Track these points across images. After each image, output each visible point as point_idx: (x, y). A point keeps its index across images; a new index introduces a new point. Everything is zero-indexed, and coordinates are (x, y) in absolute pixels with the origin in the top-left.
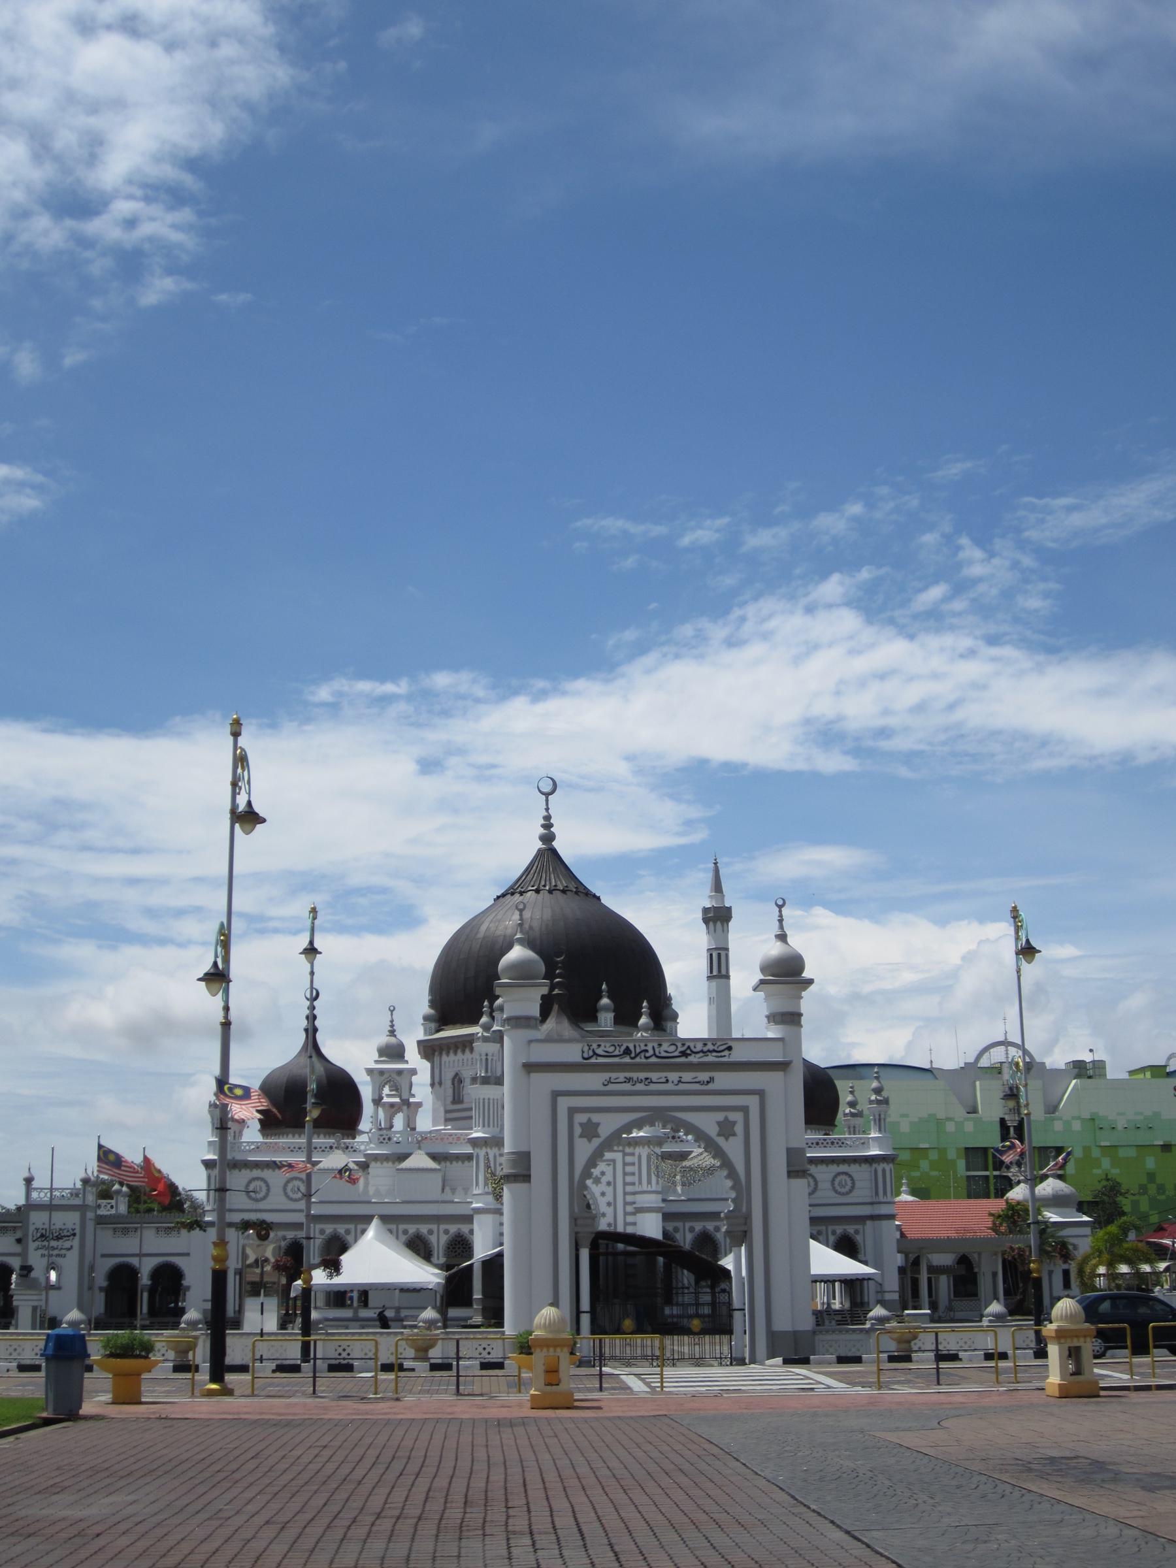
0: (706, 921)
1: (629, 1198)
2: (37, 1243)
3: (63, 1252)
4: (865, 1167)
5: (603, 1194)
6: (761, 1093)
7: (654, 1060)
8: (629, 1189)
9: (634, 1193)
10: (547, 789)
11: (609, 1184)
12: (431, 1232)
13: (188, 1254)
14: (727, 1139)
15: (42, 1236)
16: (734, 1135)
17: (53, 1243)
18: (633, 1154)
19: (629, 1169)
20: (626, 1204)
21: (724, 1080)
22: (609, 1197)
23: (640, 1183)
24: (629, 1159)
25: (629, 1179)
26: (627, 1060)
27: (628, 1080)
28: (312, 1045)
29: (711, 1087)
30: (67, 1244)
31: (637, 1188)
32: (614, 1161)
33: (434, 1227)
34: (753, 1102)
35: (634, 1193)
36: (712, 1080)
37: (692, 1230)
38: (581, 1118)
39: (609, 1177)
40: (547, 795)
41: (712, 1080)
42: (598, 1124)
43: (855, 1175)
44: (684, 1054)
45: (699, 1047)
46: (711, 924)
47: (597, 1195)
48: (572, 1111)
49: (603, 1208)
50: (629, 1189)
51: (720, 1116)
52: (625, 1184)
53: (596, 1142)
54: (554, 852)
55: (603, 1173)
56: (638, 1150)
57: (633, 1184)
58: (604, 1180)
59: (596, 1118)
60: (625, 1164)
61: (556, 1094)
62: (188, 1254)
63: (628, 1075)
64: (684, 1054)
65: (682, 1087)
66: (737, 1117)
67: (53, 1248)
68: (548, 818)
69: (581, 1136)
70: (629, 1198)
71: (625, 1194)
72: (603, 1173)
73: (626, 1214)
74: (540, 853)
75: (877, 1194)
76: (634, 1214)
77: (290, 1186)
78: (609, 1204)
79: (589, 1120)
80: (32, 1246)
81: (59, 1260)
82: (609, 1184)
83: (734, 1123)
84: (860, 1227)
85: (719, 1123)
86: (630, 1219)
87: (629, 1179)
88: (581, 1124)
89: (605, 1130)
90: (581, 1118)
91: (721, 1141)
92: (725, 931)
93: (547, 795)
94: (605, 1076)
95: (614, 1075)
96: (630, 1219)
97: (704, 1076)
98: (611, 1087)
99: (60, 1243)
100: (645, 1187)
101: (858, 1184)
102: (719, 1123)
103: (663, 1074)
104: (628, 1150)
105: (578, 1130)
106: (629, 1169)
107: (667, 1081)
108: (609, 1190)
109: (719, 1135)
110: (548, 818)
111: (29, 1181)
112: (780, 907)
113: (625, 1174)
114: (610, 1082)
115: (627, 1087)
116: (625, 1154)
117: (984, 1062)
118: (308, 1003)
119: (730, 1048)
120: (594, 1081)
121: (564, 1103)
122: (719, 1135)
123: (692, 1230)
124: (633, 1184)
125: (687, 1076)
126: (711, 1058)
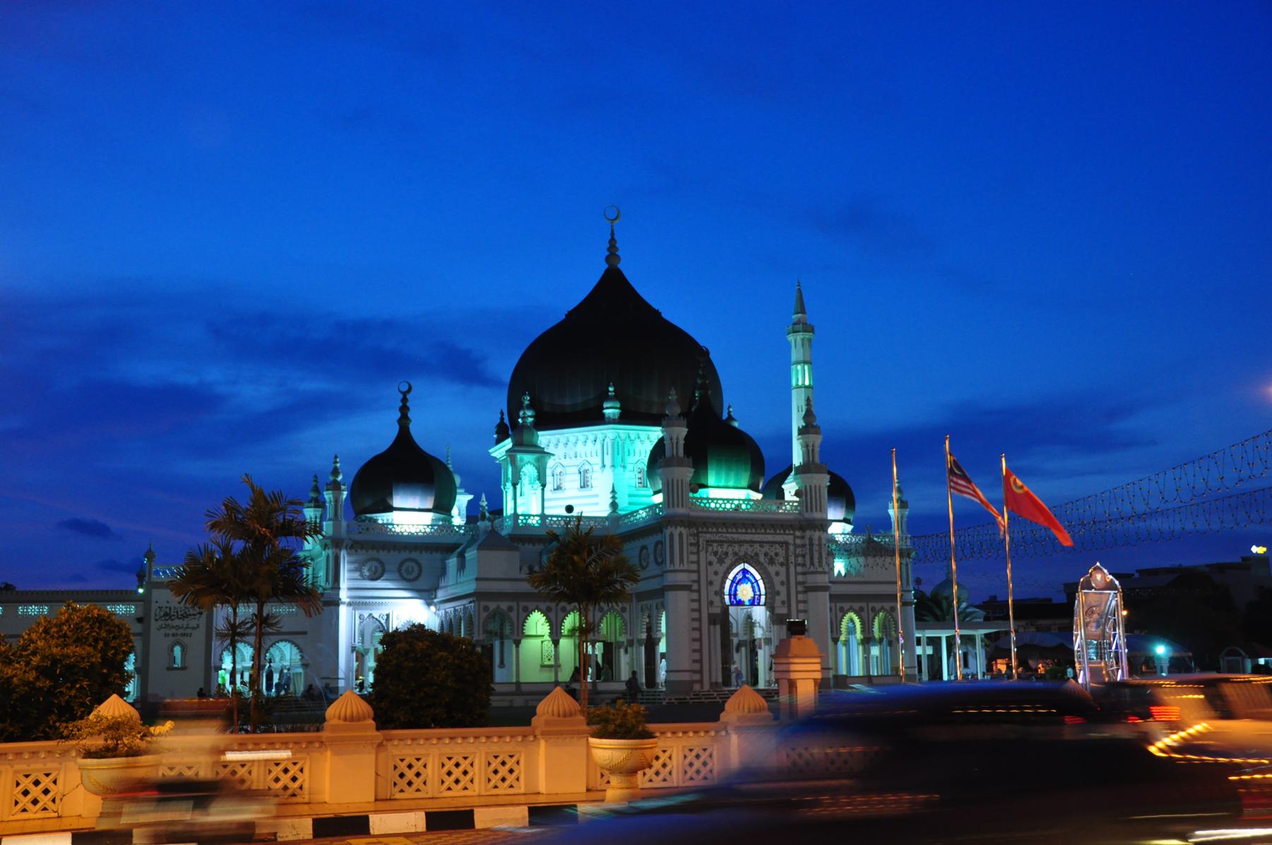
1: (800, 578)
2: (160, 622)
3: (188, 631)
9: (804, 574)
12: (510, 609)
13: (305, 633)
15: (166, 614)
17: (177, 622)
20: (798, 583)
22: (783, 577)
23: (812, 564)
28: (404, 436)
30: (193, 623)
32: (787, 543)
33: (514, 604)
35: (804, 574)
47: (773, 574)
55: (777, 554)
56: (808, 533)
62: (305, 633)
67: (178, 627)
71: (797, 574)
73: (797, 593)
74: (607, 272)
77: (416, 569)
78: (782, 583)
80: (154, 625)
81: (186, 640)
82: (782, 564)
86: (801, 597)
96: (801, 597)
99: (185, 622)
104: (798, 533)
106: (799, 551)
108: (783, 570)
116: (796, 537)
118: (401, 396)
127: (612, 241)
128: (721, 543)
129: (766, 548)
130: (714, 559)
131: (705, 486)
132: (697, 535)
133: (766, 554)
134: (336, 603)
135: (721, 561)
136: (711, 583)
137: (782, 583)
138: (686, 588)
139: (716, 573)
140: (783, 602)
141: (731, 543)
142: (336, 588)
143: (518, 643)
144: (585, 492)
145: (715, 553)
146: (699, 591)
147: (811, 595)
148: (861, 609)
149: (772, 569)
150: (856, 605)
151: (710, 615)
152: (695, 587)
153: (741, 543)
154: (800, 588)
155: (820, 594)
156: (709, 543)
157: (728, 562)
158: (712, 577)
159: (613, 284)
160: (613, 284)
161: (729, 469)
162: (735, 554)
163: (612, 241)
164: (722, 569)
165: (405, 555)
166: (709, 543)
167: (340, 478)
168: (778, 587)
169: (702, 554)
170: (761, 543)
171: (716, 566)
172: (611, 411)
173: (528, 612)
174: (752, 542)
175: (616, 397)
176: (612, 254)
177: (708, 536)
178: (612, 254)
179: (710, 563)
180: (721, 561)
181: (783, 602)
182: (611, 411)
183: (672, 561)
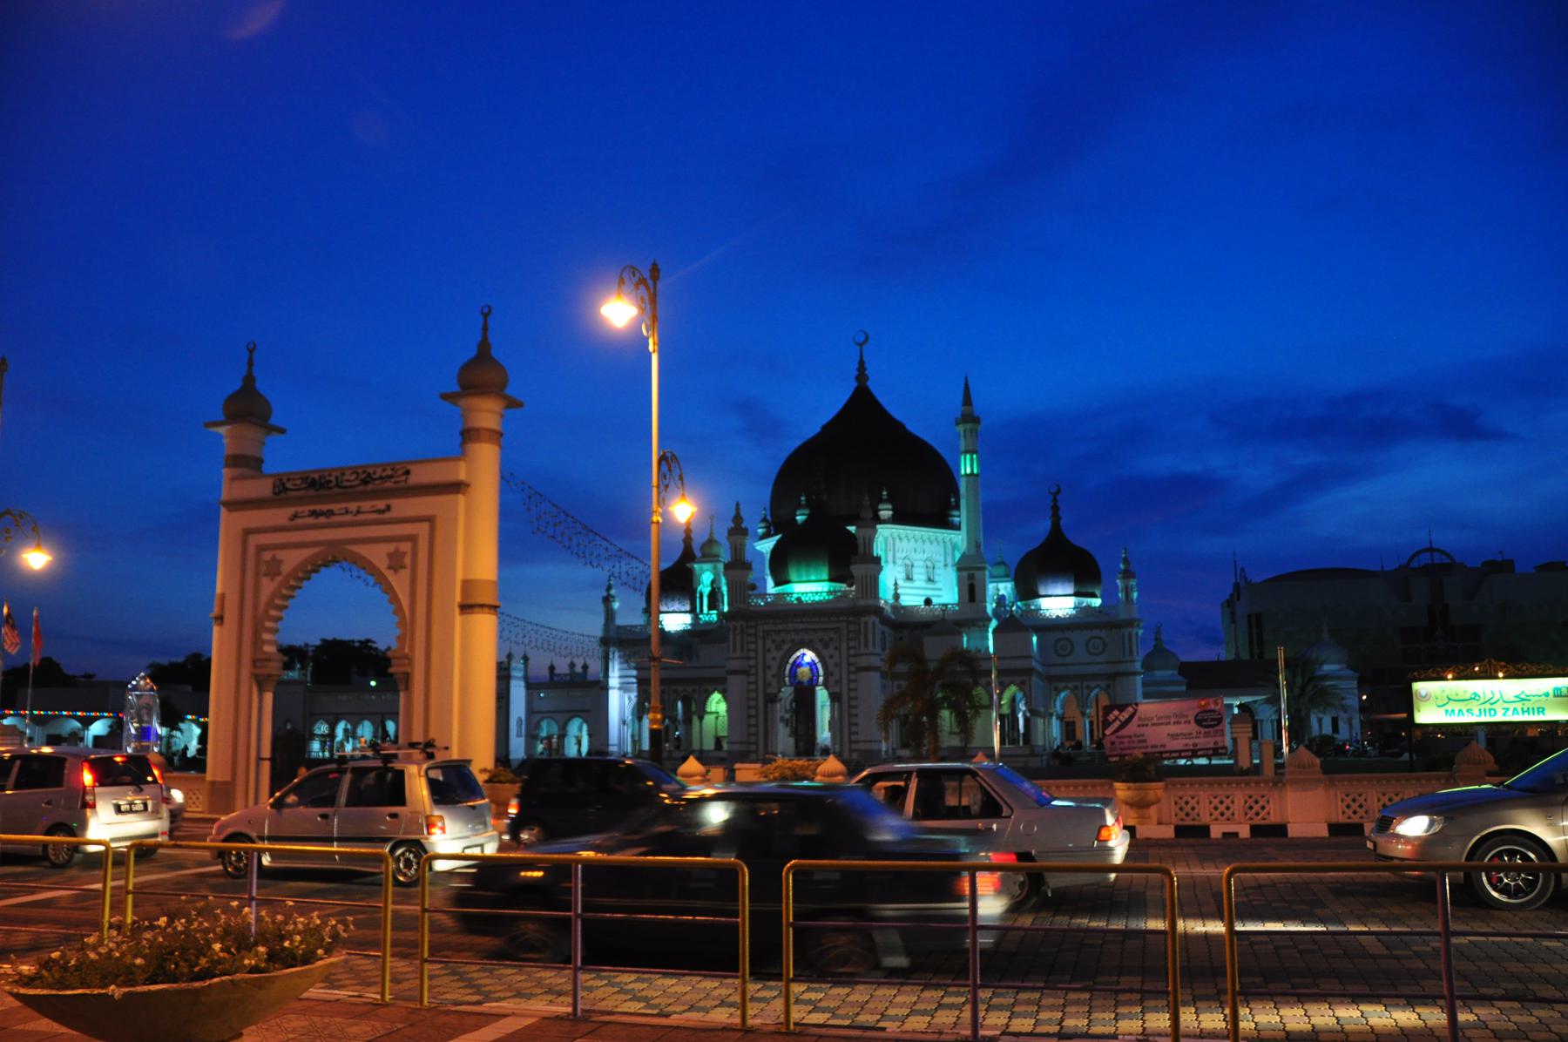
1: (852, 660)
6: (430, 520)
7: (336, 490)
14: (396, 571)
16: (403, 567)
21: (402, 507)
26: (312, 492)
27: (314, 514)
29: (387, 515)
34: (422, 529)
36: (388, 508)
38: (267, 556)
40: (861, 345)
41: (388, 508)
42: (280, 562)
44: (364, 482)
45: (379, 472)
48: (261, 549)
51: (390, 547)
53: (278, 579)
58: (832, 646)
59: (280, 554)
61: (248, 532)
63: (312, 508)
64: (364, 482)
65: (361, 517)
66: (406, 546)
69: (266, 575)
70: (852, 660)
73: (849, 673)
79: (274, 557)
83: (404, 553)
85: (390, 555)
86: (853, 677)
88: (267, 562)
89: (286, 568)
90: (267, 556)
91: (390, 575)
93: (861, 345)
94: (291, 511)
95: (299, 509)
97: (381, 504)
98: (299, 521)
100: (863, 650)
102: (390, 555)
103: (344, 505)
105: (263, 569)
107: (347, 512)
108: (836, 654)
109: (390, 568)
112: (486, 316)
114: (295, 516)
115: (311, 520)
117: (1415, 564)
119: (407, 472)
120: (280, 516)
121: (254, 540)
122: (390, 568)
125: (366, 505)
126: (389, 484)
127: (862, 363)
128: (778, 632)
131: (788, 582)
134: (605, 688)
135: (778, 648)
138: (745, 672)
141: (788, 631)
142: (606, 676)
143: (701, 718)
144: (908, 584)
148: (1023, 683)
149: (826, 653)
150: (1019, 679)
153: (797, 631)
155: (864, 674)
157: (786, 647)
158: (769, 662)
159: (862, 403)
160: (862, 403)
161: (808, 565)
163: (862, 363)
164: (779, 654)
165: (1059, 635)
167: (613, 592)
168: (831, 669)
169: (760, 643)
170: (815, 631)
171: (774, 653)
172: (886, 513)
173: (710, 693)
175: (889, 500)
176: (862, 374)
177: (766, 627)
178: (862, 374)
180: (778, 648)
182: (886, 513)
183: (866, 645)
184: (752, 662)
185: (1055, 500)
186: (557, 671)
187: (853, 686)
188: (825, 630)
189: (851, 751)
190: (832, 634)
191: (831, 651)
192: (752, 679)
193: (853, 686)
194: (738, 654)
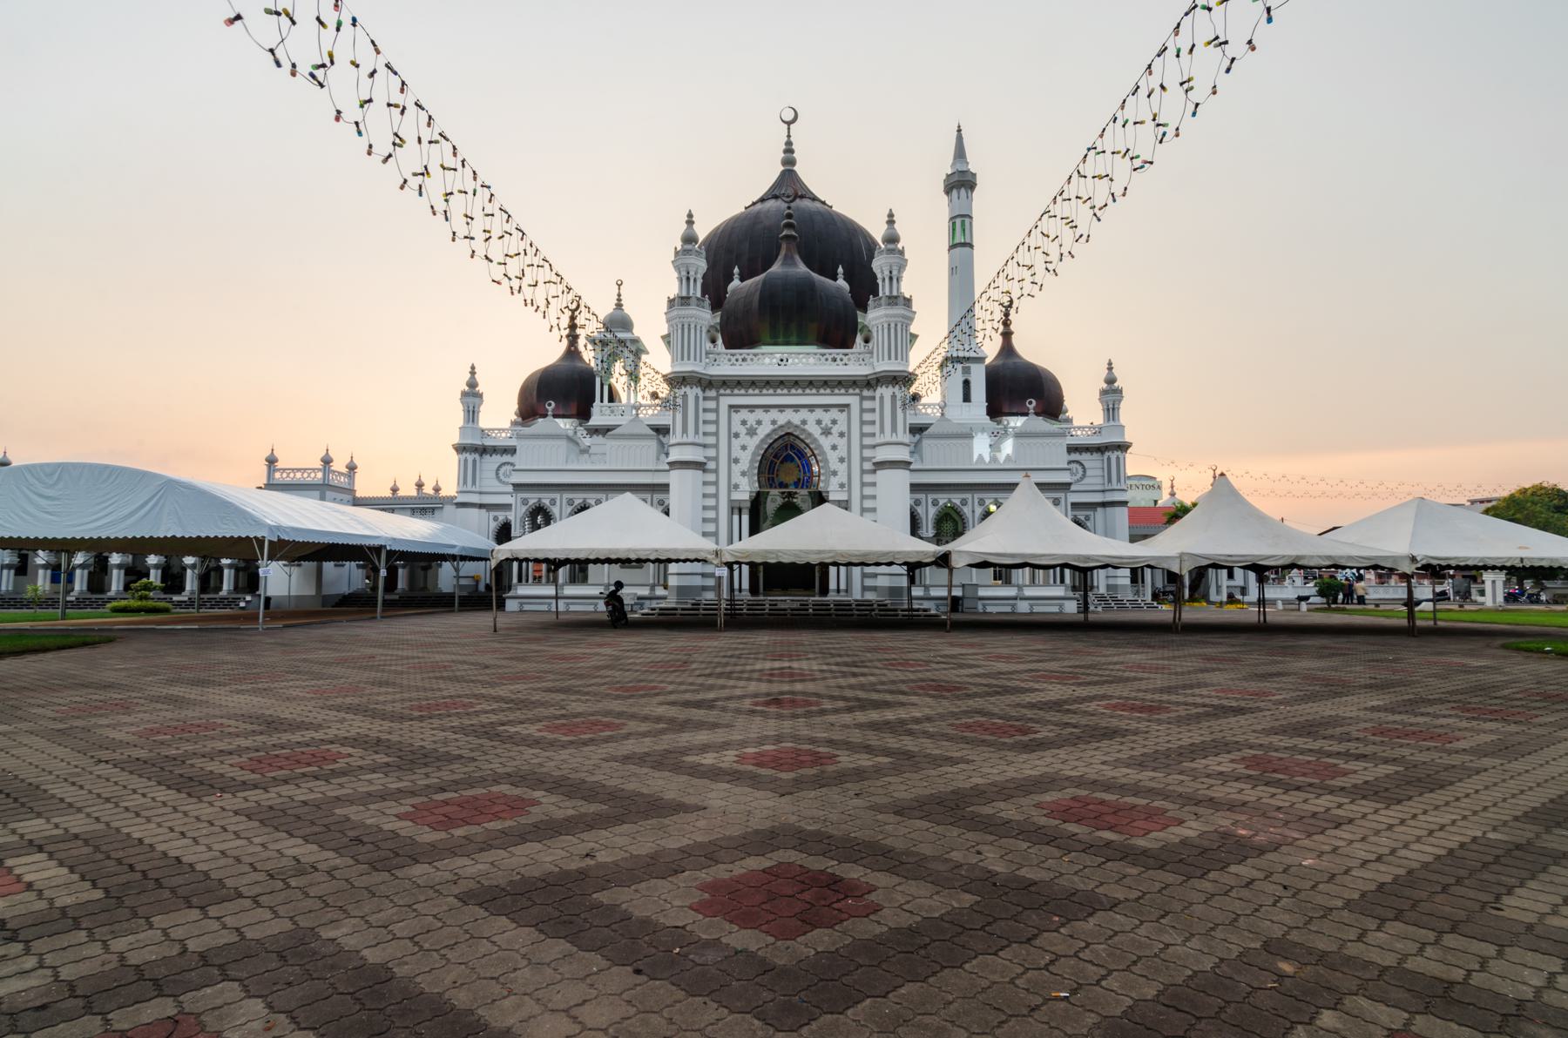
0: (948, 190)
1: (867, 453)
4: (1096, 456)
5: (834, 448)
8: (867, 441)
10: (789, 116)
11: (842, 435)
18: (873, 398)
19: (867, 417)
20: (863, 459)
23: (882, 431)
24: (867, 404)
25: (867, 429)
31: (878, 440)
32: (848, 406)
37: (935, 503)
39: (841, 427)
40: (789, 123)
43: (1087, 465)
46: (955, 192)
49: (834, 464)
50: (867, 441)
52: (863, 435)
54: (792, 172)
56: (881, 391)
57: (873, 435)
58: (835, 430)
60: (862, 411)
68: (789, 143)
70: (867, 453)
71: (863, 447)
72: (834, 422)
73: (863, 472)
74: (783, 174)
75: (1110, 481)
76: (874, 472)
78: (842, 460)
82: (842, 435)
84: (1091, 513)
86: (868, 478)
87: (867, 429)
92: (969, 198)
93: (789, 123)
100: (888, 437)
101: (1089, 473)
104: (866, 393)
106: (867, 417)
110: (789, 143)
111: (271, 461)
113: (863, 423)
116: (863, 398)
123: (935, 503)
124: (873, 435)
128: (752, 408)
129: (819, 413)
130: (743, 430)
132: (716, 399)
133: (819, 422)
136: (736, 461)
137: (842, 460)
138: (699, 466)
139: (744, 448)
140: (842, 486)
141: (767, 408)
145: (744, 423)
146: (716, 471)
147: (882, 475)
151: (731, 501)
152: (711, 465)
153: (782, 408)
154: (868, 466)
156: (734, 408)
159: (788, 185)
162: (774, 422)
166: (734, 408)
170: (811, 408)
171: (744, 439)
174: (796, 408)
179: (737, 435)
181: (842, 486)
184: (711, 453)
185: (1007, 315)
186: (400, 493)
187: (868, 491)
188: (826, 407)
189: (864, 589)
190: (834, 413)
191: (834, 439)
192: (711, 477)
193: (868, 491)
194: (691, 439)
